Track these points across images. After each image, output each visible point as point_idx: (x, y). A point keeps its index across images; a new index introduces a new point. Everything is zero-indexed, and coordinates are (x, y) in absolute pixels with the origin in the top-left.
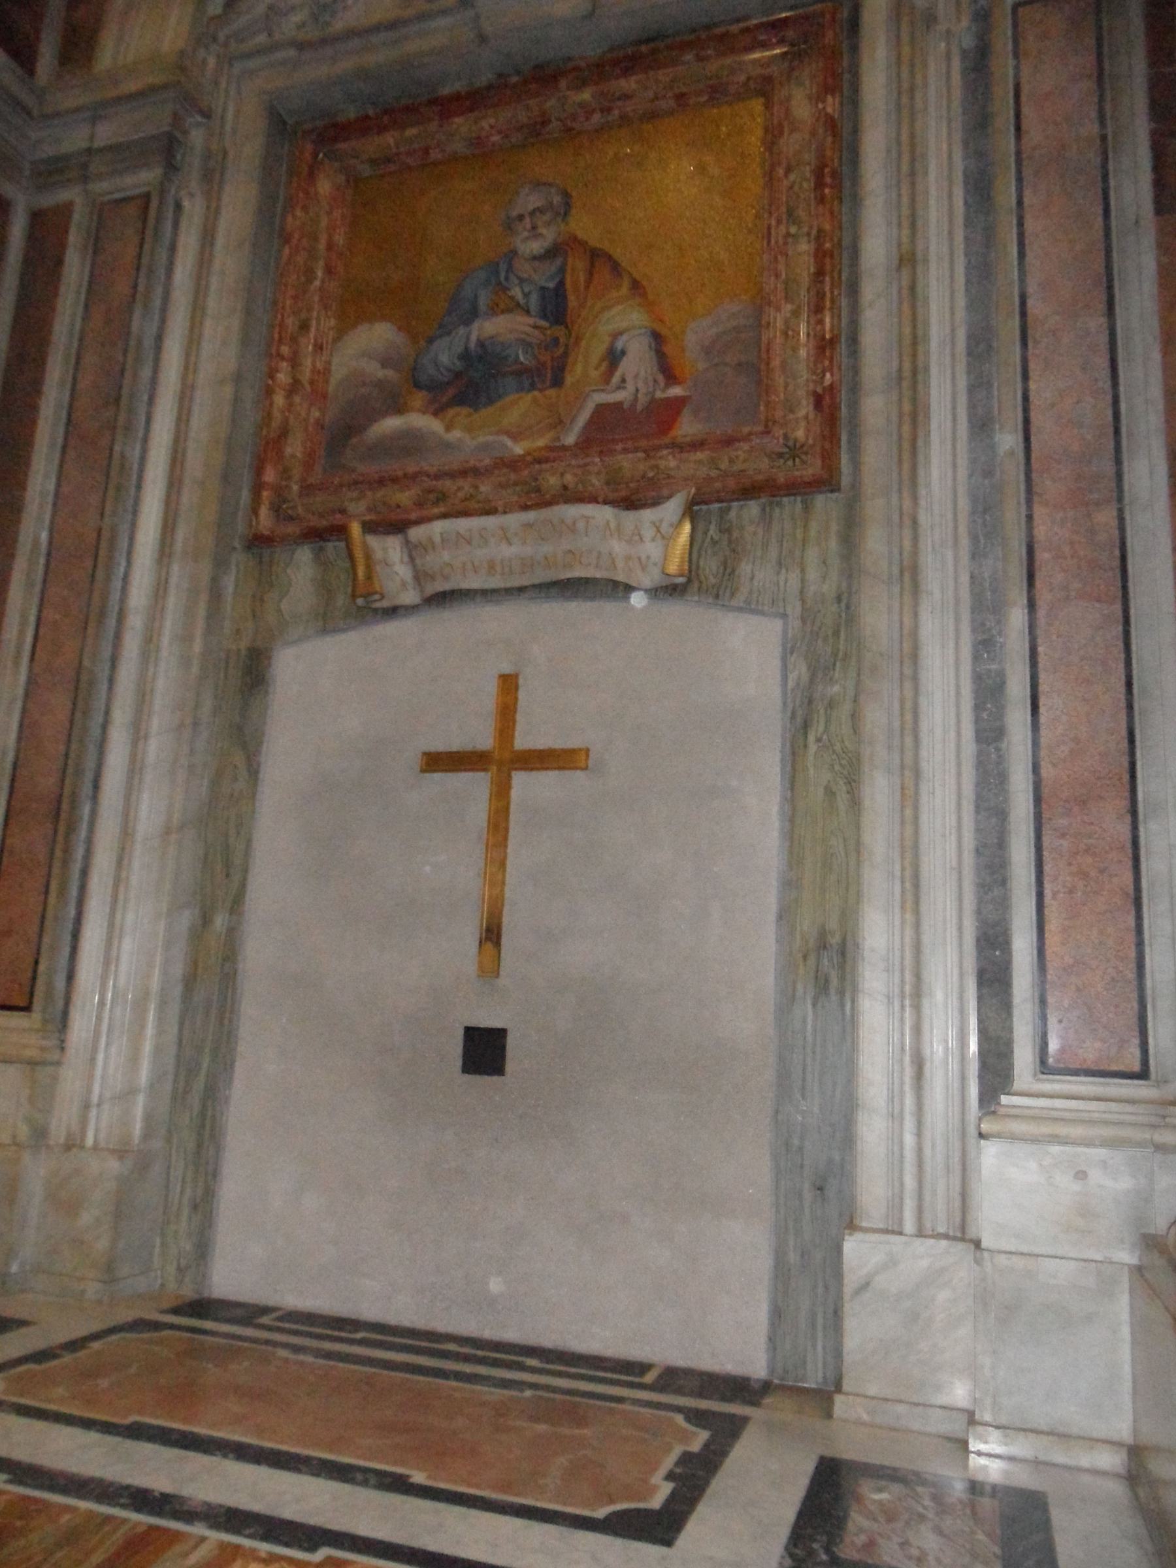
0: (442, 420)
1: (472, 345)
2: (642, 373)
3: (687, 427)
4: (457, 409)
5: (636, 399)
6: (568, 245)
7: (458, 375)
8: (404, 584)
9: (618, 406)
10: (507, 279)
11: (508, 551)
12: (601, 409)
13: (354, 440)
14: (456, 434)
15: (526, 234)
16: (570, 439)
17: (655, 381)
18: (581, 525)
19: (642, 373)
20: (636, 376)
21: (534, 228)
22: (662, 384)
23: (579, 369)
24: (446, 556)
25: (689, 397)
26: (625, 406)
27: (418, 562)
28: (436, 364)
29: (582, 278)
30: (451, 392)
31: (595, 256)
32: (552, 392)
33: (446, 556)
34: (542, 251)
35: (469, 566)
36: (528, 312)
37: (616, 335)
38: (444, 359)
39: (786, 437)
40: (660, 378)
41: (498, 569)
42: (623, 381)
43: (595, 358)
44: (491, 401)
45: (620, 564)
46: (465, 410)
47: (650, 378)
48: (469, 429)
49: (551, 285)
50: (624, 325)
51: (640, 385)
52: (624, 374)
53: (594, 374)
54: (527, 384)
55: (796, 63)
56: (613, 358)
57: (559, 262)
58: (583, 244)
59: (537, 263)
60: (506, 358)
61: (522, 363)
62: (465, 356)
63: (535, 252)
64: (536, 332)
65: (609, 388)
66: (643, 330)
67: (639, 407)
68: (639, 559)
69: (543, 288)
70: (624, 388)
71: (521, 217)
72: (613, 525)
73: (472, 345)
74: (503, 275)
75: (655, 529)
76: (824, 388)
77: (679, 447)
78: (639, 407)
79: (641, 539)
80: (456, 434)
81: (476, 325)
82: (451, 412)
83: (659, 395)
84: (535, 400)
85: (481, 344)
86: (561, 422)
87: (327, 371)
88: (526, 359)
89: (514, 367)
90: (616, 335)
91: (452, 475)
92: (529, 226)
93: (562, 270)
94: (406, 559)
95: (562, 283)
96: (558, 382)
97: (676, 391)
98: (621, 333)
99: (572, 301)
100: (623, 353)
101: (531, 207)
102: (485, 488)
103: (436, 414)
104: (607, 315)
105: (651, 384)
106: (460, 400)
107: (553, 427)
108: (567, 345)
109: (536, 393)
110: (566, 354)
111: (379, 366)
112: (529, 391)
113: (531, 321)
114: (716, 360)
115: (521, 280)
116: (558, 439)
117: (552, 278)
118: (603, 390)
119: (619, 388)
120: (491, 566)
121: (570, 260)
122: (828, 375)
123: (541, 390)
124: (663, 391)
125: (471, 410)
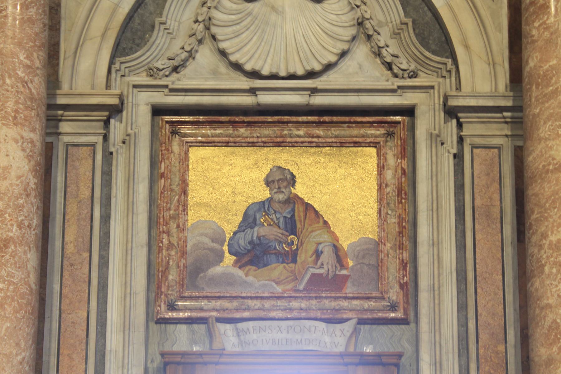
0: (243, 271)
1: (255, 238)
2: (330, 263)
3: (349, 289)
4: (250, 267)
5: (328, 274)
6: (295, 199)
7: (249, 251)
8: (234, 345)
9: (322, 274)
10: (269, 210)
11: (279, 336)
12: (313, 275)
13: (201, 275)
14: (250, 279)
15: (275, 190)
16: (301, 287)
17: (336, 267)
18: (313, 329)
19: (330, 263)
20: (328, 263)
21: (279, 188)
22: (339, 268)
23: (303, 256)
24: (255, 336)
25: (350, 275)
26: (324, 275)
27: (242, 338)
28: (238, 243)
29: (302, 214)
30: (246, 259)
31: (308, 207)
32: (292, 265)
33: (255, 336)
34: (284, 199)
35: (265, 341)
36: (279, 227)
37: (319, 244)
38: (242, 242)
39: (389, 298)
40: (338, 265)
41: (277, 342)
42: (322, 264)
43: (310, 253)
44: (265, 265)
45: (328, 344)
46: (254, 268)
47: (334, 265)
48: (255, 276)
49: (289, 216)
50: (322, 240)
51: (330, 267)
52: (322, 262)
53: (310, 260)
54: (281, 260)
55: (388, 139)
56: (318, 254)
57: (292, 205)
58: (301, 199)
59: (281, 205)
60: (270, 247)
61: (278, 250)
62: (251, 242)
63: (281, 199)
64: (284, 238)
65: (316, 267)
66: (330, 244)
67: (330, 277)
68: (335, 343)
69: (285, 217)
70: (323, 268)
71: (273, 181)
72: (325, 330)
73: (255, 238)
74: (266, 207)
75: (341, 333)
76: (404, 283)
77: (346, 298)
78: (330, 277)
79: (336, 336)
80: (250, 279)
81: (256, 229)
82: (247, 268)
83: (338, 273)
84: (285, 267)
85: (259, 238)
86: (297, 279)
87: (186, 241)
88: (279, 248)
89: (274, 252)
90: (319, 244)
91: (251, 298)
92: (277, 187)
93: (293, 210)
94: (235, 334)
95: (293, 216)
96: (294, 261)
97: (344, 272)
98: (320, 243)
99: (299, 225)
100: (322, 252)
101: (277, 178)
102: (268, 304)
103: (240, 267)
104: (314, 234)
105: (334, 268)
106: (251, 262)
107: (293, 280)
108: (297, 245)
109: (285, 264)
110: (297, 249)
111: (210, 241)
112: (282, 263)
113: (281, 231)
114: (361, 261)
115: (275, 212)
116: (296, 286)
117: (289, 213)
118: (314, 268)
119: (320, 267)
120: (274, 341)
121: (296, 206)
122: (405, 278)
123: (287, 264)
124: (339, 271)
125: (257, 269)
